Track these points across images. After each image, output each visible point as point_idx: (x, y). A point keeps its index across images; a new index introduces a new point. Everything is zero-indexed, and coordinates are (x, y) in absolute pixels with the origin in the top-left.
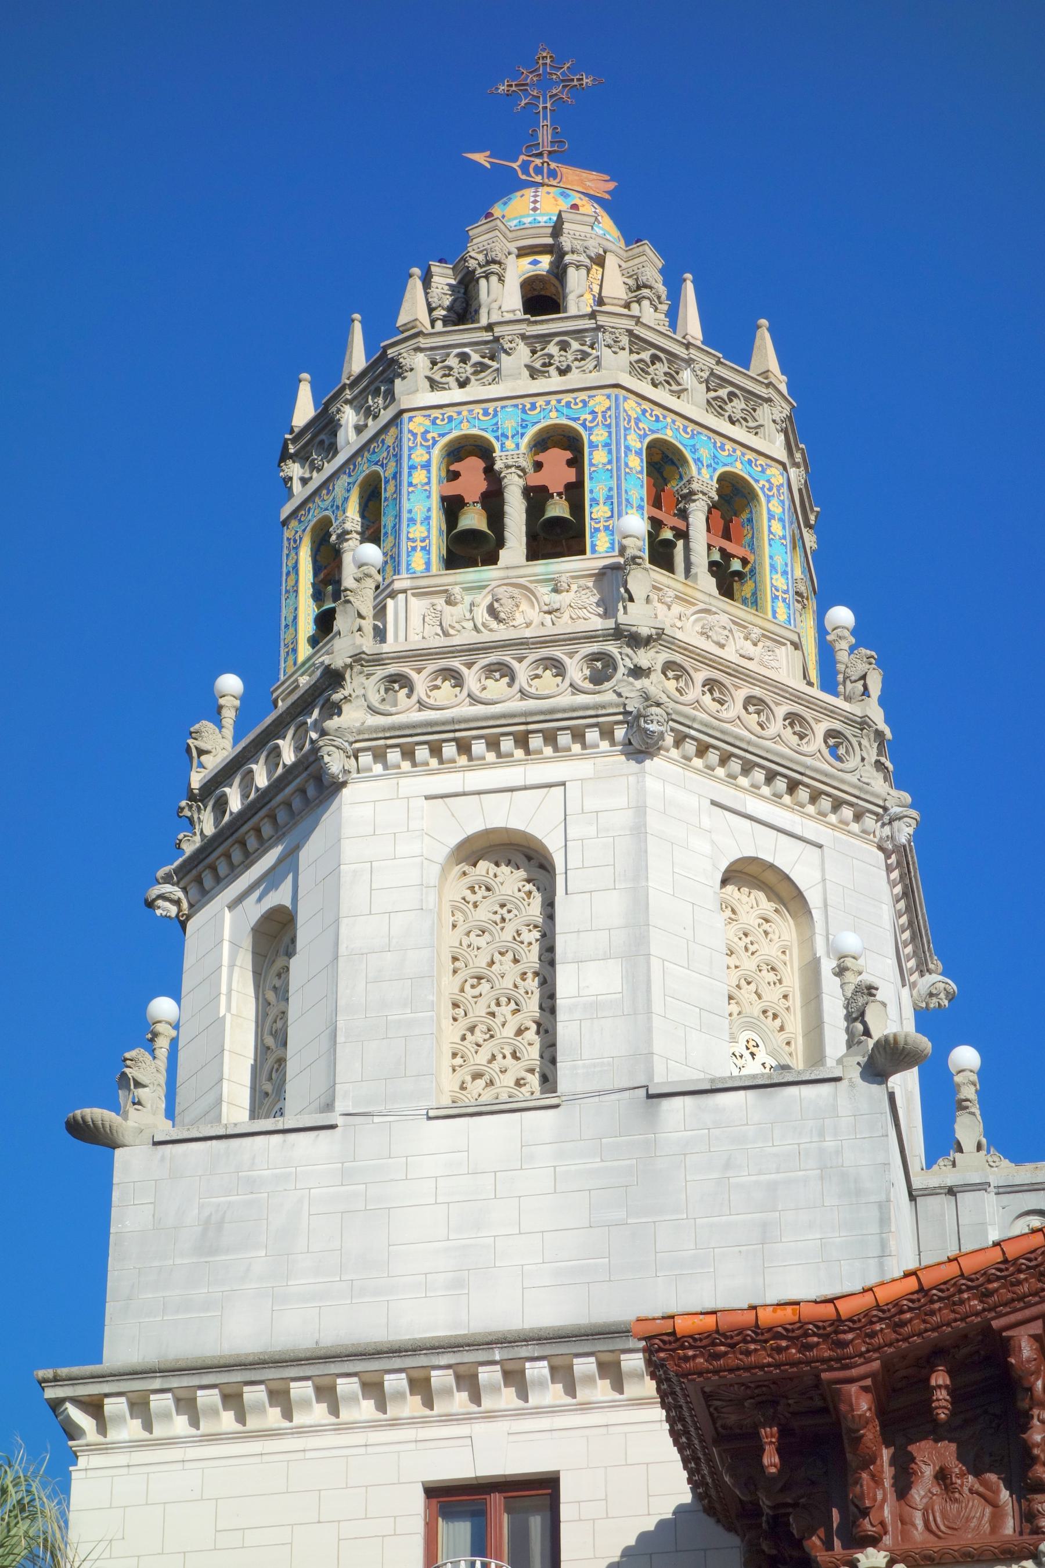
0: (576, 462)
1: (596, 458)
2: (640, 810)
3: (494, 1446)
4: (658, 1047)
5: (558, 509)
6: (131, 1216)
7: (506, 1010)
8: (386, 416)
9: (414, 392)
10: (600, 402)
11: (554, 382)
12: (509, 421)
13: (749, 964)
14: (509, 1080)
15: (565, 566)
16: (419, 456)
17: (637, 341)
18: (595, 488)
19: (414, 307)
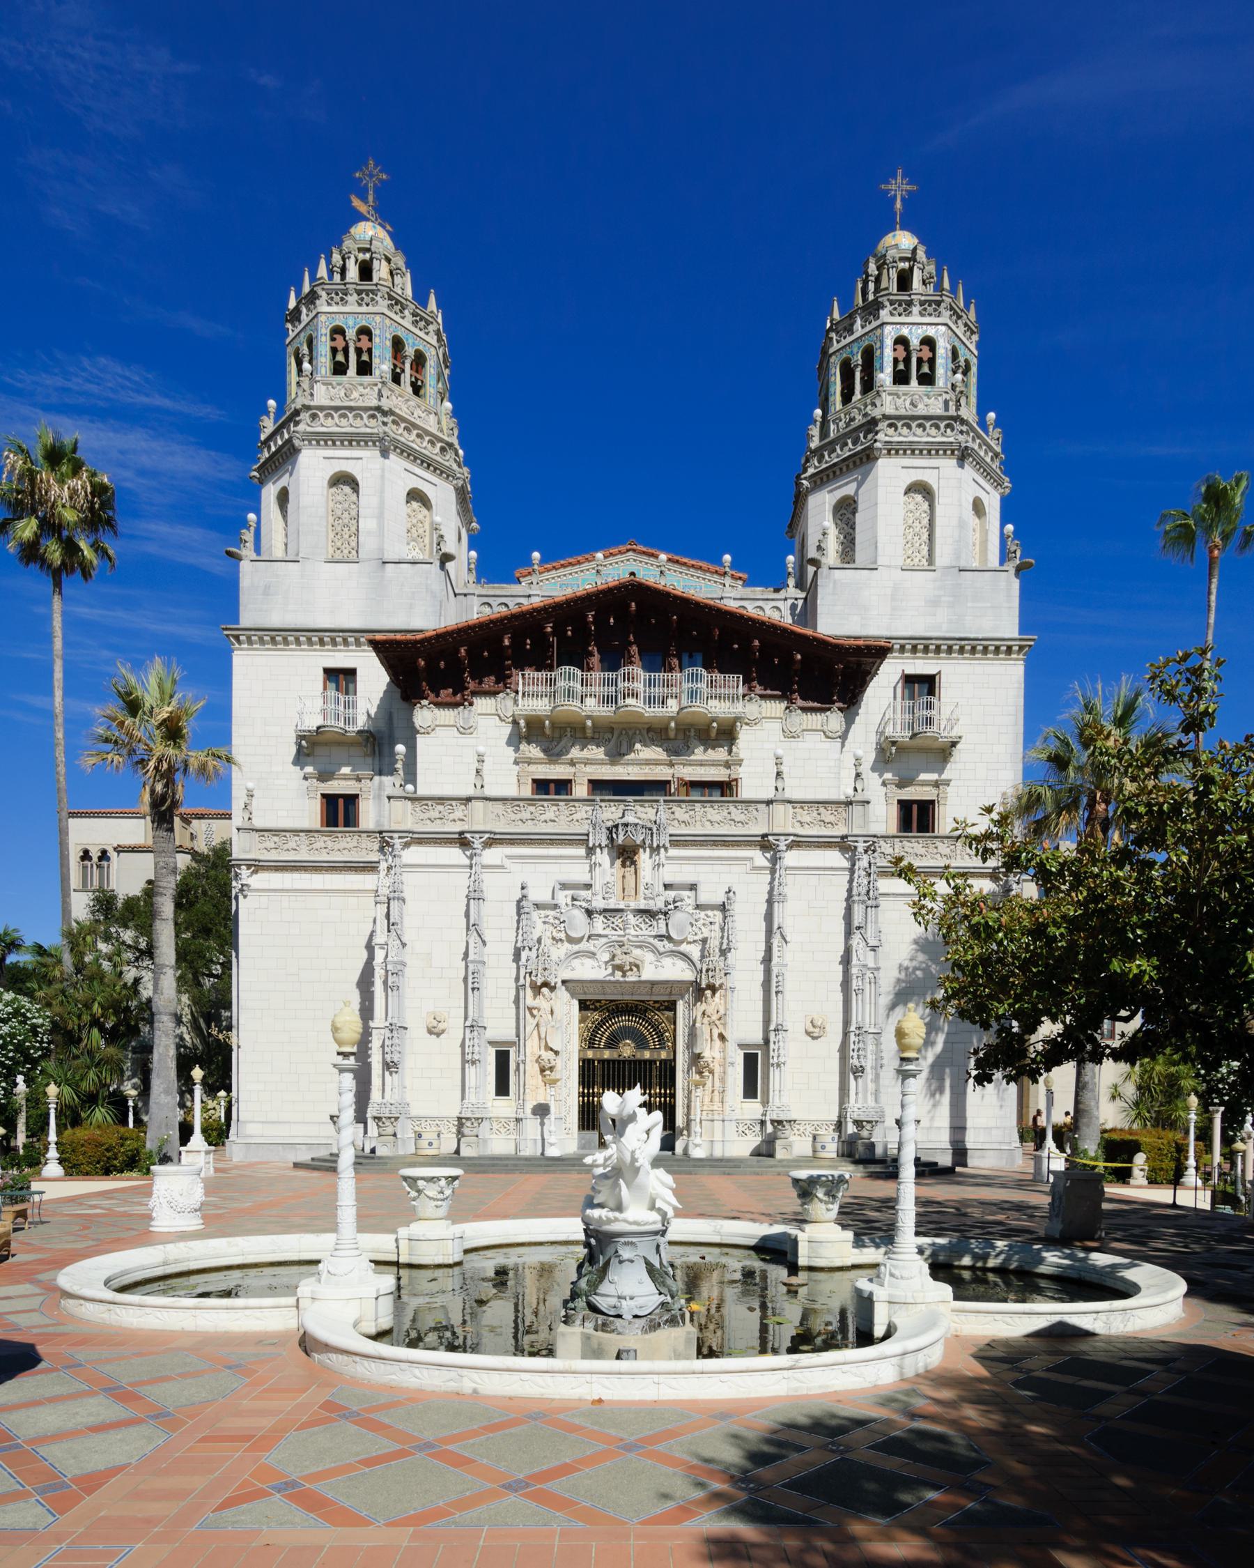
0: (370, 340)
1: (376, 340)
2: (383, 470)
3: (340, 659)
4: (386, 546)
5: (365, 357)
6: (245, 582)
7: (346, 529)
8: (314, 313)
9: (322, 306)
10: (378, 318)
11: (364, 309)
12: (351, 323)
13: (415, 521)
14: (346, 552)
15: (366, 379)
16: (324, 331)
17: (391, 298)
18: (375, 352)
19: (322, 271)
